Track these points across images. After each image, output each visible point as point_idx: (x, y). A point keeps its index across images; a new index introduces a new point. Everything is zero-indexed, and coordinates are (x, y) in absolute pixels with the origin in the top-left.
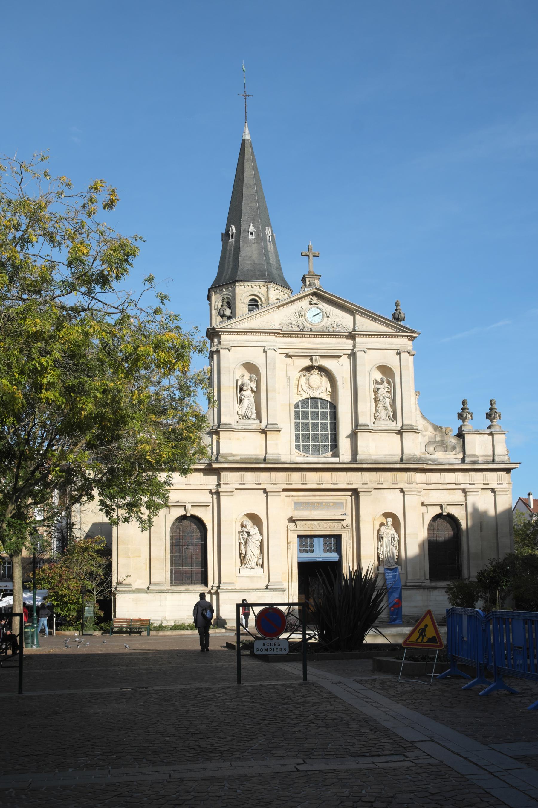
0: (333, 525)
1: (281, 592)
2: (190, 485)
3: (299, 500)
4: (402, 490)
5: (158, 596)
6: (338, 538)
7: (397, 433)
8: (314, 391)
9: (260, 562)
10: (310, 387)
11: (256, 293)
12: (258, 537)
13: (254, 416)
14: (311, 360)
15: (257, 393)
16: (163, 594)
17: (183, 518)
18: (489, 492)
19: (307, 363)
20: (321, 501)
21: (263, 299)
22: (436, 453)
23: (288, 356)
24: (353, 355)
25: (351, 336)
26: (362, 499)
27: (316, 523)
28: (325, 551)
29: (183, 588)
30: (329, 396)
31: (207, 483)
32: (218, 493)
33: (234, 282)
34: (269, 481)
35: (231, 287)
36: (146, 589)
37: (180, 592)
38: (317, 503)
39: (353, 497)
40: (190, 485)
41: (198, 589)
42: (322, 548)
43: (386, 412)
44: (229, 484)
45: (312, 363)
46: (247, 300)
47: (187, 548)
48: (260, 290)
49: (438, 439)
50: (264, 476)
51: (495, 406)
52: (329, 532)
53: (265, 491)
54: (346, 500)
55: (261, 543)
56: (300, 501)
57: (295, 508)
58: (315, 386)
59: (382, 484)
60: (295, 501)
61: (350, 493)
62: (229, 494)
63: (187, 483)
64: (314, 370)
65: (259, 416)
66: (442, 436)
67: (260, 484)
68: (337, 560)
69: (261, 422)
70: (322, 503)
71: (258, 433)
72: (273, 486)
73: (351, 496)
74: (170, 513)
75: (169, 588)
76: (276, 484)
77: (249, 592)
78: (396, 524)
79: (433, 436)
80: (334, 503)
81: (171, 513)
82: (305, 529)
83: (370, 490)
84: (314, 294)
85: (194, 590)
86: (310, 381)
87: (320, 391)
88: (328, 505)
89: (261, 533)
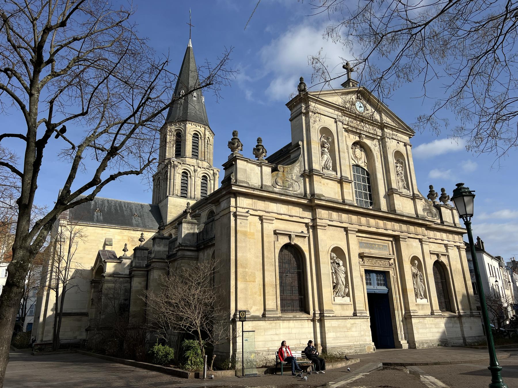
0: (384, 263)
1: (366, 320)
2: (292, 216)
3: (362, 240)
4: (421, 241)
5: (274, 323)
6: (385, 274)
7: (412, 199)
8: (358, 161)
9: (347, 290)
10: (356, 157)
11: (198, 130)
12: (343, 268)
13: (331, 169)
14: (360, 137)
15: (332, 152)
16: (278, 321)
17: (287, 247)
18: (456, 248)
19: (357, 139)
20: (375, 243)
21: (202, 135)
22: (428, 217)
23: (347, 130)
24: (382, 140)
25: (382, 126)
26: (403, 244)
27: (374, 260)
28: (378, 284)
29: (291, 315)
30: (366, 167)
31: (304, 216)
32: (314, 227)
33: (187, 120)
34: (347, 221)
35: (183, 123)
36: (261, 316)
37: (289, 319)
38: (373, 244)
39: (394, 242)
40: (292, 216)
41: (303, 316)
42: (376, 282)
43: (403, 183)
44: (323, 219)
45: (360, 139)
46: (192, 133)
47: (286, 276)
48: (201, 129)
49: (428, 208)
50: (344, 216)
51: (445, 192)
52: (382, 268)
53: (346, 230)
54: (388, 244)
55: (346, 273)
56: (363, 241)
57: (360, 247)
58: (358, 157)
59: (410, 234)
60: (360, 241)
61: (391, 239)
62: (323, 228)
63: (290, 214)
64: (358, 146)
65: (334, 169)
66: (429, 206)
67: (342, 223)
68: (386, 293)
69: (337, 174)
70: (375, 244)
71: (336, 182)
72: (350, 225)
73: (391, 241)
74: (278, 241)
75: (280, 315)
76: (352, 224)
77: (346, 319)
78: (420, 267)
79: (425, 205)
80: (382, 245)
81: (279, 240)
82: (370, 265)
83: (406, 237)
84: (358, 92)
85: (299, 317)
86: (356, 153)
87: (361, 161)
88: (379, 247)
89: (345, 265)
